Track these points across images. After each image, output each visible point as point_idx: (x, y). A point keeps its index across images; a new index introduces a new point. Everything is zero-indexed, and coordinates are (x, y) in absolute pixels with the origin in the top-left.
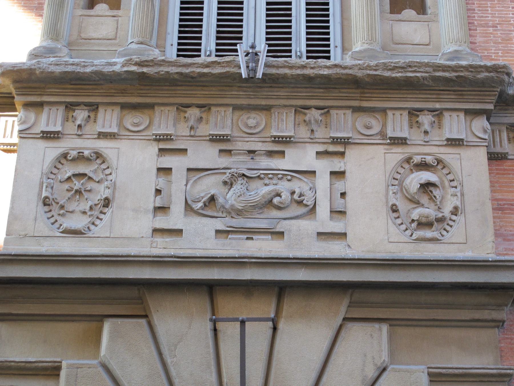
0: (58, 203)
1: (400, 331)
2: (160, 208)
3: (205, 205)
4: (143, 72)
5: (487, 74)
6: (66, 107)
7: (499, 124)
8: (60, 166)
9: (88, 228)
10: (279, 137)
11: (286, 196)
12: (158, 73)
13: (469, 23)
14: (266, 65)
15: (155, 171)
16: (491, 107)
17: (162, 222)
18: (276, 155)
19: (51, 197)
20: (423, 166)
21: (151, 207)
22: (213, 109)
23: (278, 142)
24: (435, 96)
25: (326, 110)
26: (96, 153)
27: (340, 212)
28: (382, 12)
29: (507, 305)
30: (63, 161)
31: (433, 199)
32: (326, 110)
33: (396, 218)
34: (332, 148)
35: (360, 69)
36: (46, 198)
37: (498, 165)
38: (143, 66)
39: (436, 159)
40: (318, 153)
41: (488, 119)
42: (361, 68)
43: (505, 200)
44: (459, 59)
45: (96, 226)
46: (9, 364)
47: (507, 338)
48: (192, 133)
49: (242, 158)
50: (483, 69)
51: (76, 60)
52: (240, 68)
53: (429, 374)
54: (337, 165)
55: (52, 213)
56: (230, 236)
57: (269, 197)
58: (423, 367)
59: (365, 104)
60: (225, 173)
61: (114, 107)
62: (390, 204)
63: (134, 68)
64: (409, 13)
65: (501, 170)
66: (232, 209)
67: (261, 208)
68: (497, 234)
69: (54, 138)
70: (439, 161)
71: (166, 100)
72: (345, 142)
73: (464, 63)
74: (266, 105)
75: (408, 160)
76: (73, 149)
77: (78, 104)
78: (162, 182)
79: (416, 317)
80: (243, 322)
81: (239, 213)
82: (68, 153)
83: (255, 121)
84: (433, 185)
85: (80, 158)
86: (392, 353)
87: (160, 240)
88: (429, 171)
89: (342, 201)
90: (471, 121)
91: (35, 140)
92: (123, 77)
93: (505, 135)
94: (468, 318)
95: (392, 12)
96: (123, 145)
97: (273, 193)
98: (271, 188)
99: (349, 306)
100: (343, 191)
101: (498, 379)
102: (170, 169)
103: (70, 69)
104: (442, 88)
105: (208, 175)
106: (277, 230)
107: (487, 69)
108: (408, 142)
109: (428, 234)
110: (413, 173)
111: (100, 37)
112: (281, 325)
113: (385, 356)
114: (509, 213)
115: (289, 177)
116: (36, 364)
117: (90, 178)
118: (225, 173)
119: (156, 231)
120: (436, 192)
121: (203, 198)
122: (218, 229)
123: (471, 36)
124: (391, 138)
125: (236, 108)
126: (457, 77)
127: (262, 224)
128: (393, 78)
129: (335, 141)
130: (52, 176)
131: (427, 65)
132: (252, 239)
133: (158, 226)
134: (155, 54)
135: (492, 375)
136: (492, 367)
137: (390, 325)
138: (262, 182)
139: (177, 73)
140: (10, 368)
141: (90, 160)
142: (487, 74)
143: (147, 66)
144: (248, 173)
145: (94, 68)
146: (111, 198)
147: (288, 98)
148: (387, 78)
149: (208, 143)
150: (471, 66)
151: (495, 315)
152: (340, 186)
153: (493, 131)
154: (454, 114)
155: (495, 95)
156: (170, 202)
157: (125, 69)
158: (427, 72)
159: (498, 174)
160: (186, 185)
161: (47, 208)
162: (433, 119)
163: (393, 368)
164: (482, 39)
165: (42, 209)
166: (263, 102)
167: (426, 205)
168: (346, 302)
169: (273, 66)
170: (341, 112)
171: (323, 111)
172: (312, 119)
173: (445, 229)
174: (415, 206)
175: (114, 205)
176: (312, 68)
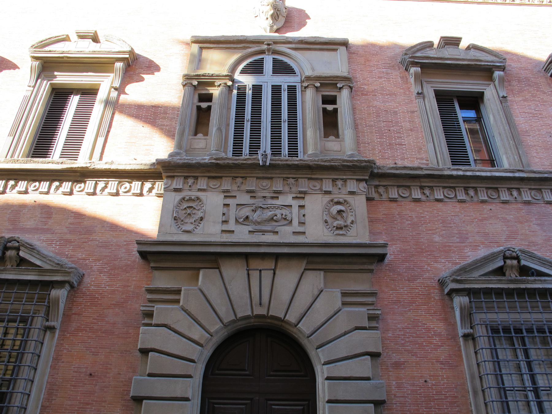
0: (180, 219)
1: (328, 274)
2: (224, 221)
3: (244, 220)
4: (218, 163)
5: (365, 164)
6: (184, 178)
7: (370, 185)
8: (181, 203)
9: (194, 230)
10: (276, 191)
11: (279, 216)
12: (224, 163)
13: (358, 142)
14: (271, 160)
15: (223, 205)
16: (367, 178)
17: (225, 227)
18: (275, 198)
19: (177, 217)
20: (338, 203)
21: (221, 220)
22: (248, 178)
23: (276, 193)
24: (343, 173)
25: (296, 179)
26: (197, 197)
27: (303, 223)
28: (320, 137)
29: (374, 263)
30: (183, 201)
31: (342, 217)
32: (296, 179)
33: (327, 226)
34: (299, 195)
35: (311, 161)
36: (175, 217)
37: (371, 203)
38: (217, 160)
39: (344, 200)
40: (293, 197)
41: (366, 183)
42: (311, 161)
43: (374, 218)
44: (353, 157)
45: (197, 229)
46: (159, 289)
47: (374, 277)
48: (239, 189)
49: (260, 200)
50: (364, 162)
51: (189, 158)
52: (259, 161)
53: (342, 293)
54: (302, 203)
55: (178, 223)
56: (255, 233)
57: (272, 217)
58: (338, 290)
59: (313, 176)
60: (253, 206)
61: (205, 178)
62: (324, 219)
63: (213, 161)
64: (332, 138)
65: (372, 205)
66: (256, 222)
67: (268, 221)
68: (370, 232)
69: (179, 191)
70: (345, 201)
71: (227, 175)
72: (305, 193)
73: (356, 159)
74: (270, 177)
75: (332, 201)
76: (187, 196)
77: (189, 177)
78: (225, 210)
79: (336, 268)
80: (260, 271)
81: (259, 223)
82: (185, 198)
83: (266, 184)
84: (343, 211)
85: (190, 200)
86: (325, 284)
87: (225, 235)
88: (341, 205)
89: (304, 218)
90: (359, 184)
91: (171, 192)
92: (209, 165)
93: (373, 189)
94: (358, 269)
95: (324, 138)
96: (209, 194)
97: (274, 215)
98: (273, 212)
99: (307, 264)
100: (304, 214)
101: (371, 295)
102: (229, 204)
103: (186, 161)
104: (346, 170)
105: (246, 207)
106: (275, 231)
107: (365, 161)
108: (332, 193)
109: (341, 232)
110: (334, 206)
111: (199, 148)
112: (277, 272)
113: (322, 285)
114: (375, 223)
115: (281, 208)
116: (171, 289)
117: (194, 208)
118: (253, 206)
119: (223, 231)
120: (344, 214)
121: (243, 217)
122: (250, 230)
123: (358, 147)
124: (324, 191)
125: (258, 178)
126: (353, 165)
127: (269, 228)
128: (325, 165)
129: (301, 192)
130: (178, 208)
131: (340, 160)
132: (264, 234)
133: (224, 229)
134: (223, 155)
135: (369, 293)
136: (369, 289)
137: (325, 272)
138: (269, 210)
139: (232, 163)
140: (159, 290)
141: (195, 200)
142: (365, 164)
143: (219, 160)
144: (263, 206)
145: (196, 161)
146: (203, 217)
147: (280, 174)
148: (322, 165)
149: (245, 194)
150: (358, 160)
151: (370, 267)
152: (302, 212)
153: (368, 188)
154: (352, 181)
155: (369, 173)
156: (229, 218)
157: (210, 161)
158: (340, 163)
159: (370, 206)
160: (236, 211)
161: (175, 221)
162: (343, 183)
163: (326, 291)
164: (363, 149)
165: (173, 222)
166: (269, 176)
167: (340, 220)
168: (305, 262)
169: (274, 160)
170: (303, 180)
171: (295, 180)
172: (291, 183)
173: (348, 230)
174: (335, 220)
176: (290, 161)
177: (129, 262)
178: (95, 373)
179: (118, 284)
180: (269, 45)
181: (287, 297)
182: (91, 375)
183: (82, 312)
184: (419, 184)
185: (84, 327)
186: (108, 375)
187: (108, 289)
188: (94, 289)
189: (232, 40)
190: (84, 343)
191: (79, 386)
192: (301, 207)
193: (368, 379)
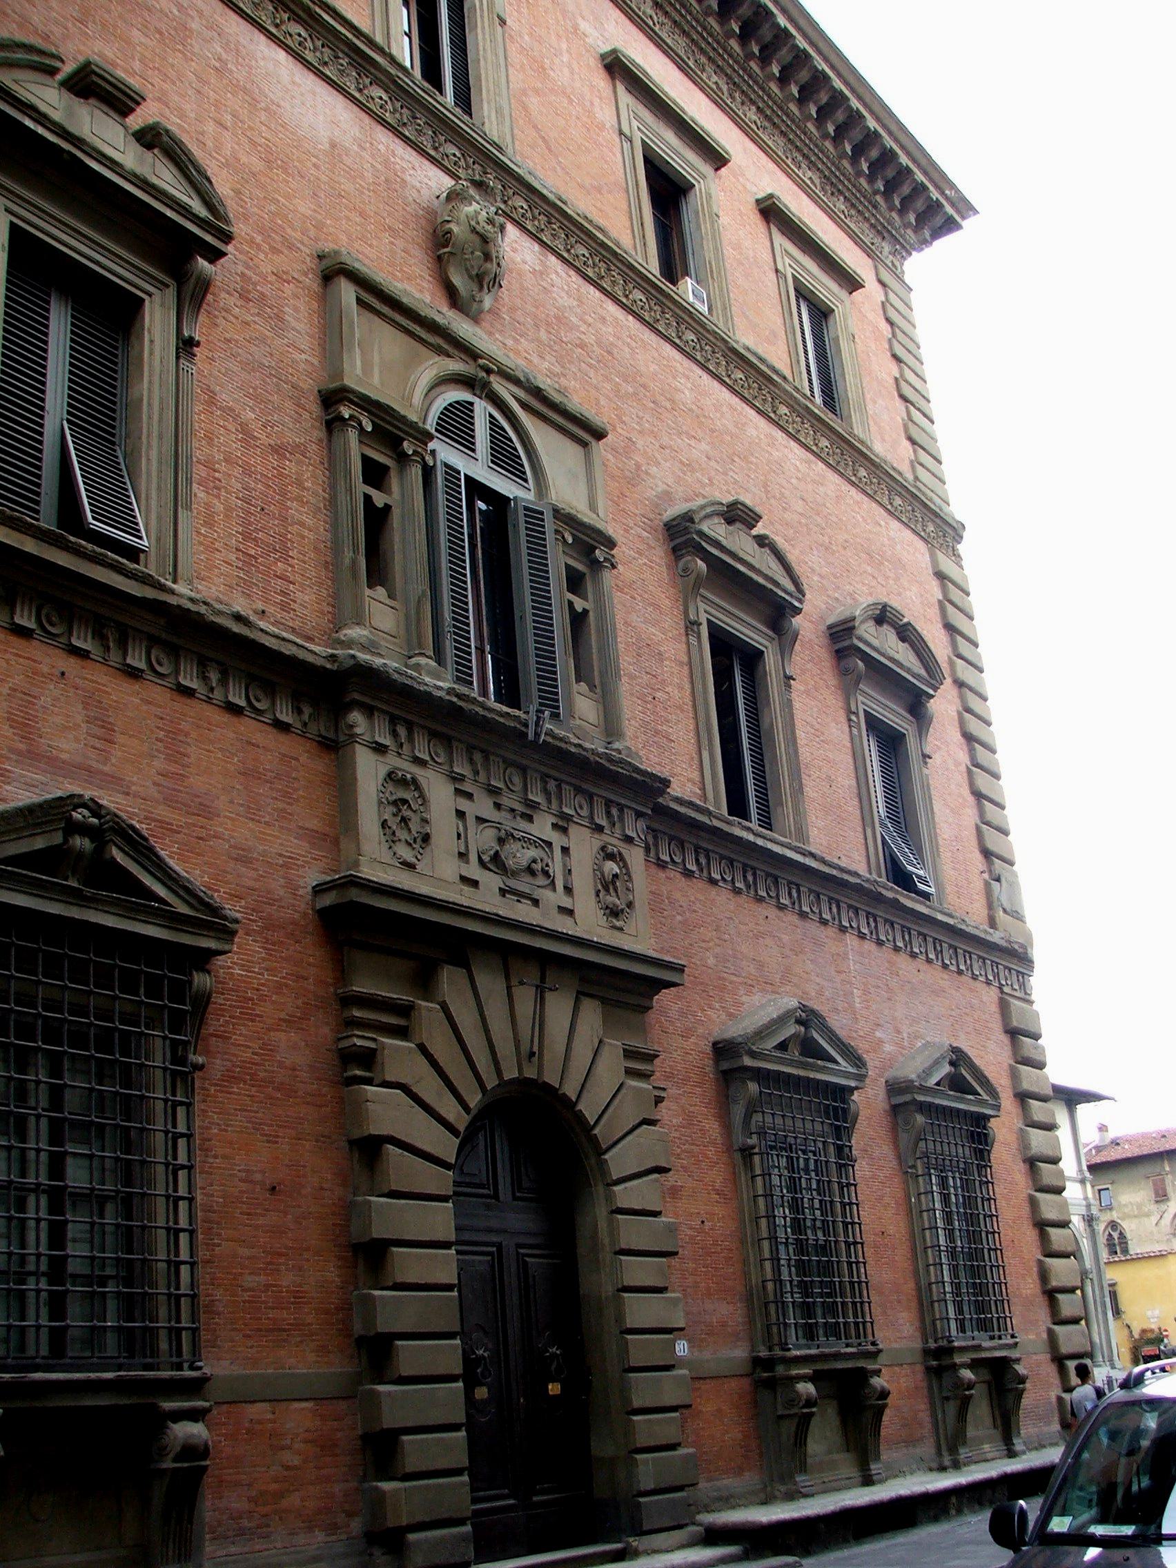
36: (386, 820)
63: (455, 699)
76: (400, 770)
82: (393, 772)
103: (409, 682)
157: (448, 697)
175: (433, 840)
176: (566, 743)
177: (296, 916)
178: (279, 1184)
179: (284, 968)
180: (489, 371)
181: (562, 1048)
182: (274, 1188)
183: (229, 1033)
184: (695, 841)
185: (239, 1072)
186: (304, 1192)
187: (268, 980)
188: (242, 975)
189: (423, 314)
190: (246, 1110)
191: (256, 1214)
192: (565, 850)
193: (655, 1214)
